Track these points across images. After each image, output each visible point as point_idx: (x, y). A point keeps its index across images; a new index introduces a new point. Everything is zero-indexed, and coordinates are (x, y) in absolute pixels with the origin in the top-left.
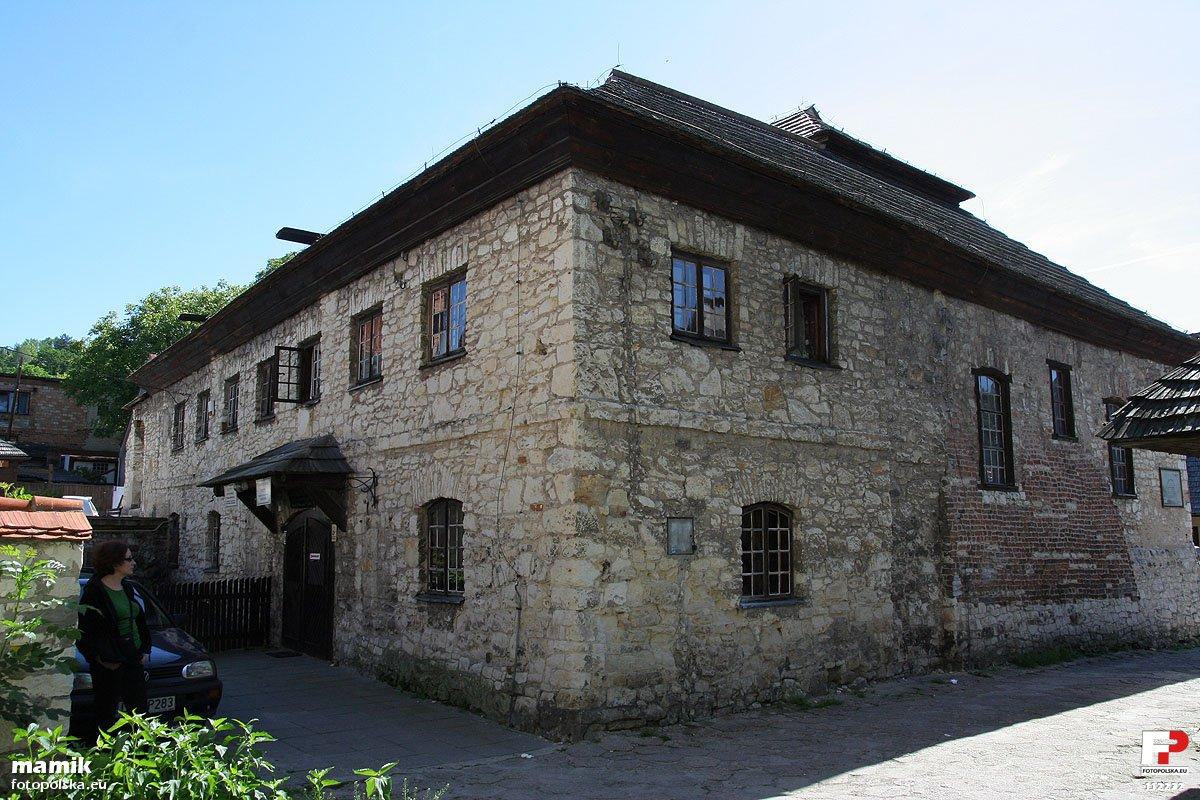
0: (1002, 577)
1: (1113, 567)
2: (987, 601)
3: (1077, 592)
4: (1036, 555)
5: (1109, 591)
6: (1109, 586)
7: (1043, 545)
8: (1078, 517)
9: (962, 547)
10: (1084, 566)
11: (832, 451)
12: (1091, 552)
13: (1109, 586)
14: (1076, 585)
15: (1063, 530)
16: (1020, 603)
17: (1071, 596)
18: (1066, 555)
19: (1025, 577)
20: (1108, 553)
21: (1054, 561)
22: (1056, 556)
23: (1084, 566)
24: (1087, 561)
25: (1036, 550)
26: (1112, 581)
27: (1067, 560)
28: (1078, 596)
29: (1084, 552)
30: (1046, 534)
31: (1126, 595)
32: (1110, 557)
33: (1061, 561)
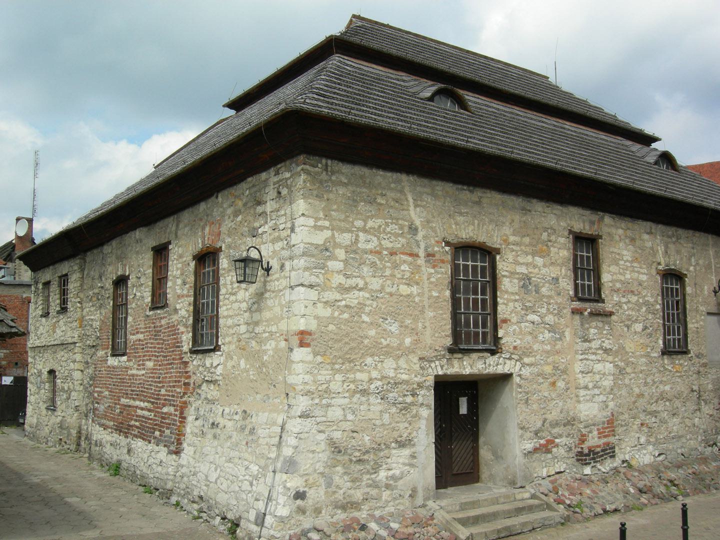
0: (105, 412)
1: (163, 418)
2: (101, 425)
3: (136, 433)
4: (124, 401)
5: (155, 438)
6: (157, 433)
7: (127, 394)
8: (152, 373)
9: (97, 392)
10: (146, 413)
11: (64, 346)
12: (153, 403)
13: (157, 433)
14: (137, 427)
15: (140, 384)
16: (110, 430)
17: (131, 434)
18: (137, 403)
19: (114, 414)
20: (164, 405)
21: (130, 406)
22: (132, 403)
23: (146, 413)
24: (149, 410)
25: (123, 397)
26: (160, 431)
27: (137, 407)
28: (136, 436)
29: (148, 402)
30: (130, 386)
31: (165, 446)
32: (165, 410)
33: (134, 407)
